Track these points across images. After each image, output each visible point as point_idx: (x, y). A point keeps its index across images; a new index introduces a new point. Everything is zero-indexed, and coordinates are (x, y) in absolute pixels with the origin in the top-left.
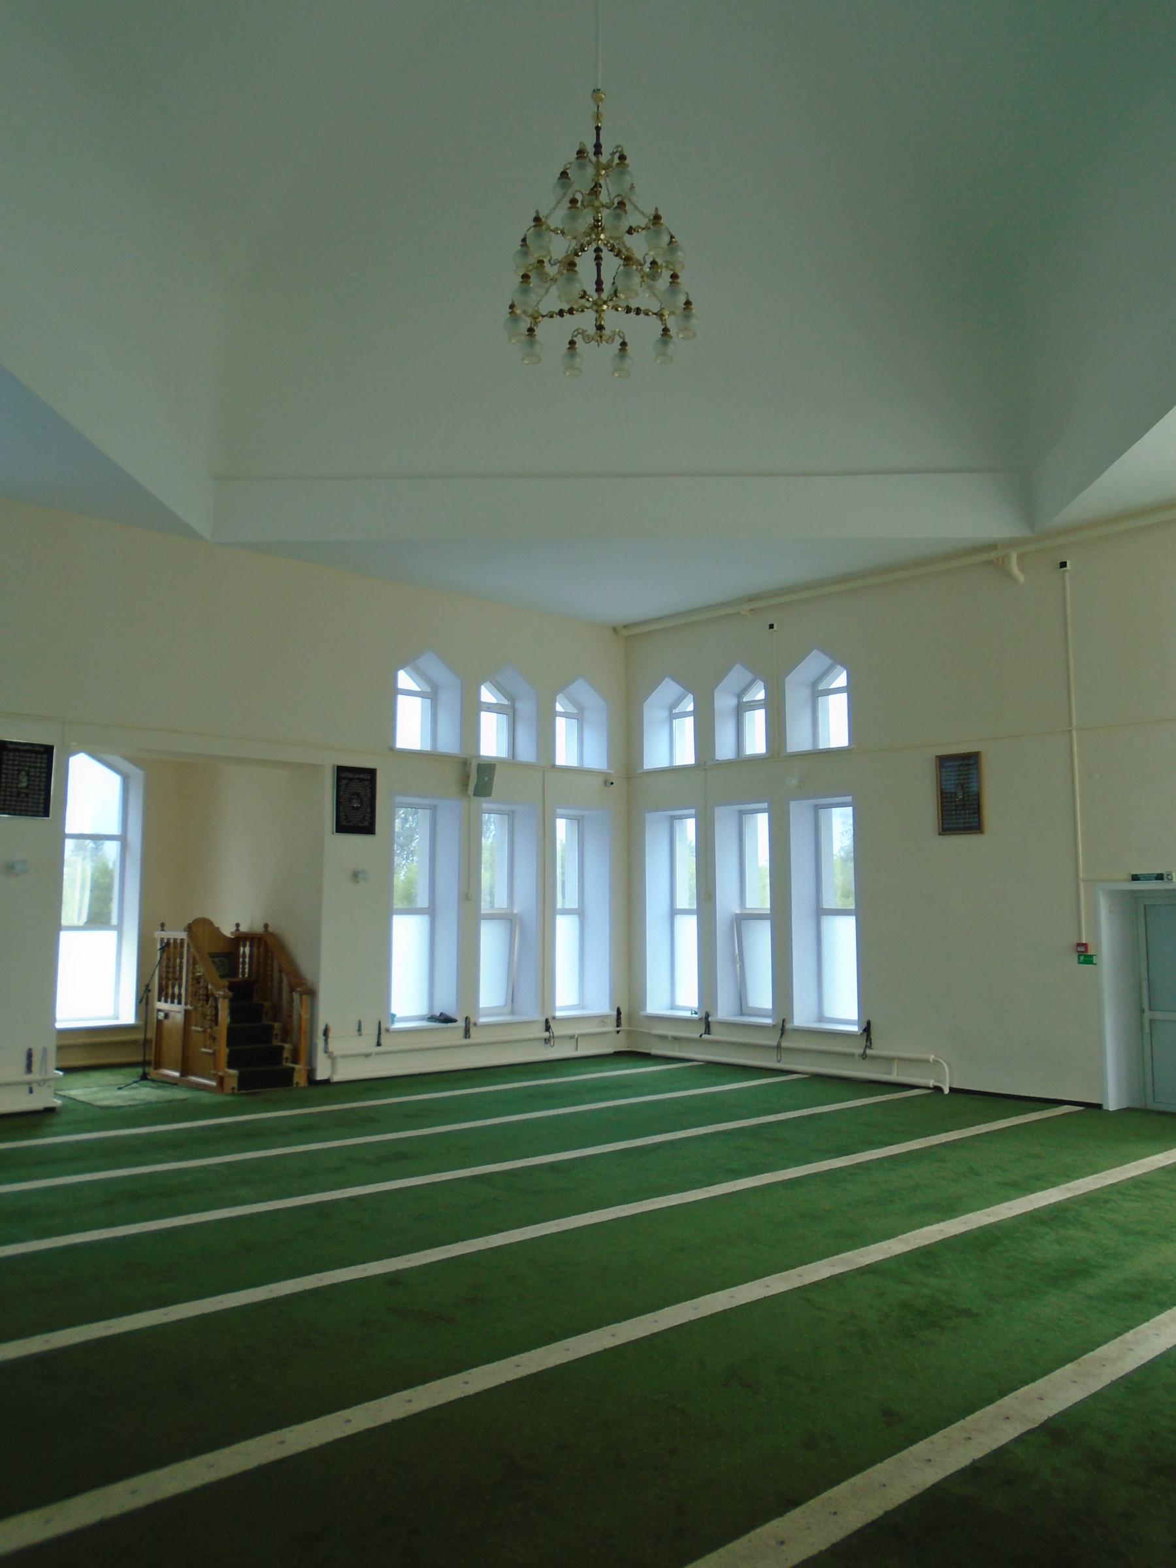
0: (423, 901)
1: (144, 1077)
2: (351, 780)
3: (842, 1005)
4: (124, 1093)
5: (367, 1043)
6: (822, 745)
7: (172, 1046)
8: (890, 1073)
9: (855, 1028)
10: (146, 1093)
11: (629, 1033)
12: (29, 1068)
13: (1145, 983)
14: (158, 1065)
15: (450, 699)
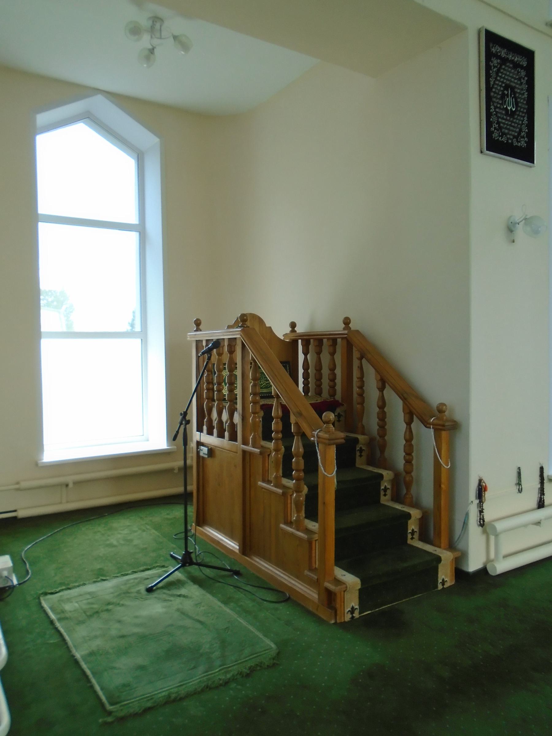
2: (504, 61)
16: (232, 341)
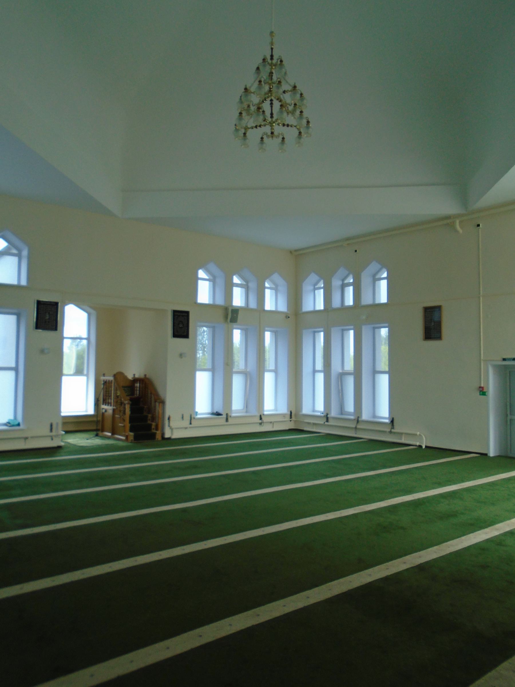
0: (209, 366)
1: (97, 435)
3: (384, 412)
4: (89, 441)
5: (186, 423)
6: (377, 302)
7: (108, 424)
8: (401, 439)
9: (387, 421)
10: (97, 442)
11: (295, 422)
12: (51, 430)
13: (508, 404)
14: (103, 431)
15: (221, 282)
16: (112, 381)
